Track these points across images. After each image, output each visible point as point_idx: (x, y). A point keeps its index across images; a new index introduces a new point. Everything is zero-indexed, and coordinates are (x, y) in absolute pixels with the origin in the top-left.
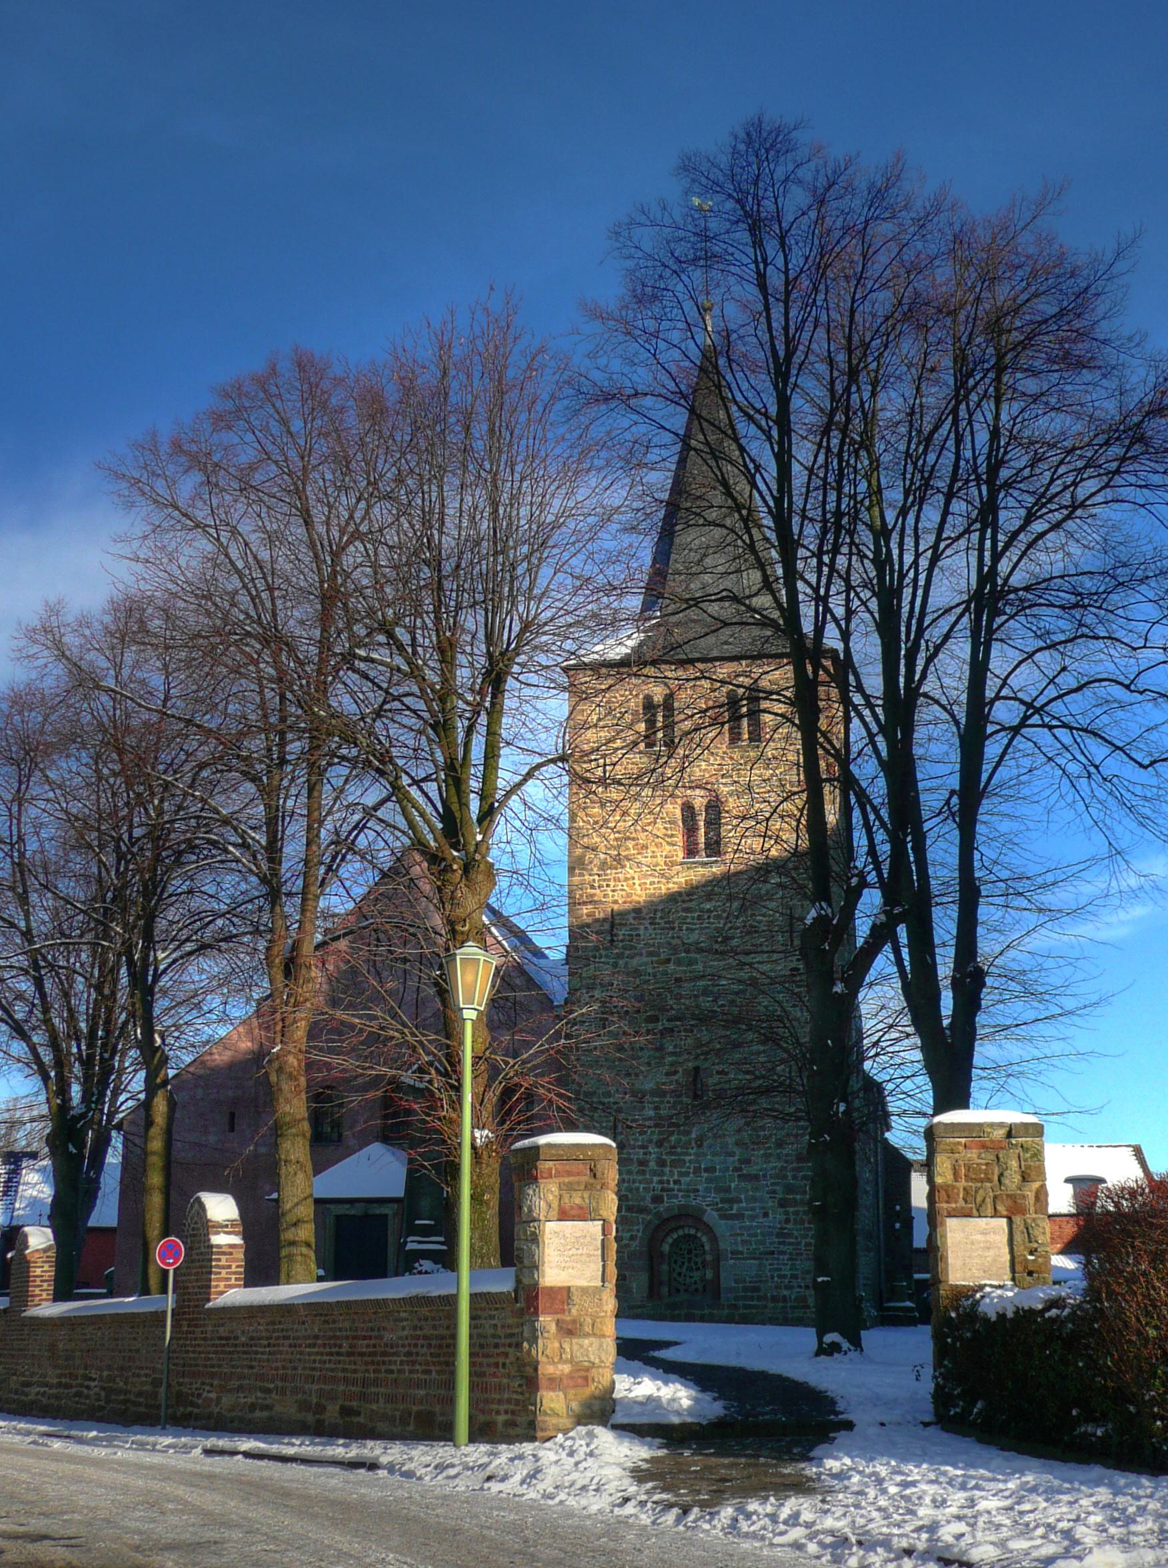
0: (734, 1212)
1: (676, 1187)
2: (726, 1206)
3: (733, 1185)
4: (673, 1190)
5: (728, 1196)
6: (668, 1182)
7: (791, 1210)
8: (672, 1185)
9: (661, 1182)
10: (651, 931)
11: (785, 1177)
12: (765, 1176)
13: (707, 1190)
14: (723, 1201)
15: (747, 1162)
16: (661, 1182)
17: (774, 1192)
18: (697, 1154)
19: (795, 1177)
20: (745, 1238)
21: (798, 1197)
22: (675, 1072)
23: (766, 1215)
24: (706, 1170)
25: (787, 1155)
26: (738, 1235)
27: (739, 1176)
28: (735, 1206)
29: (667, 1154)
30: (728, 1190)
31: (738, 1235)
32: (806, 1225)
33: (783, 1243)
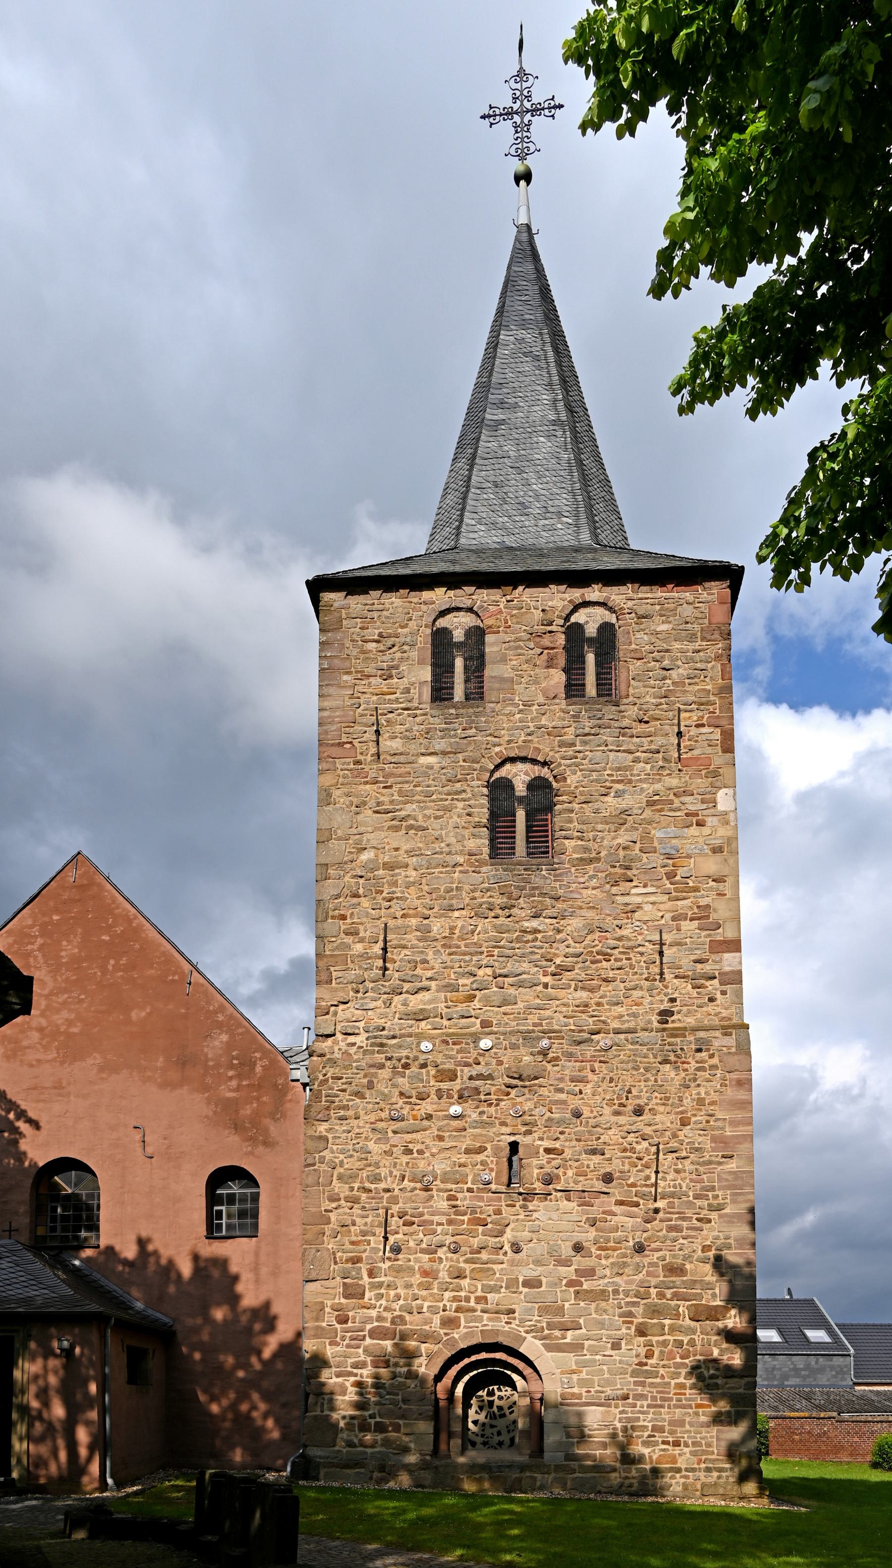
0: (568, 1340)
1: (479, 1307)
2: (557, 1333)
3: (567, 1305)
4: (474, 1310)
5: (557, 1319)
6: (467, 1299)
7: (655, 1339)
8: (472, 1303)
9: (455, 1299)
10: (445, 957)
11: (647, 1296)
12: (616, 1292)
13: (528, 1311)
14: (550, 1326)
15: (590, 1273)
16: (455, 1299)
17: (630, 1314)
18: (512, 1263)
19: (661, 1295)
20: (584, 1375)
21: (667, 1322)
22: (481, 1150)
23: (616, 1346)
24: (527, 1284)
25: (651, 1264)
26: (573, 1372)
27: (577, 1293)
28: (570, 1333)
29: (466, 1261)
30: (560, 1311)
31: (573, 1372)
32: (678, 1360)
33: (642, 1384)
